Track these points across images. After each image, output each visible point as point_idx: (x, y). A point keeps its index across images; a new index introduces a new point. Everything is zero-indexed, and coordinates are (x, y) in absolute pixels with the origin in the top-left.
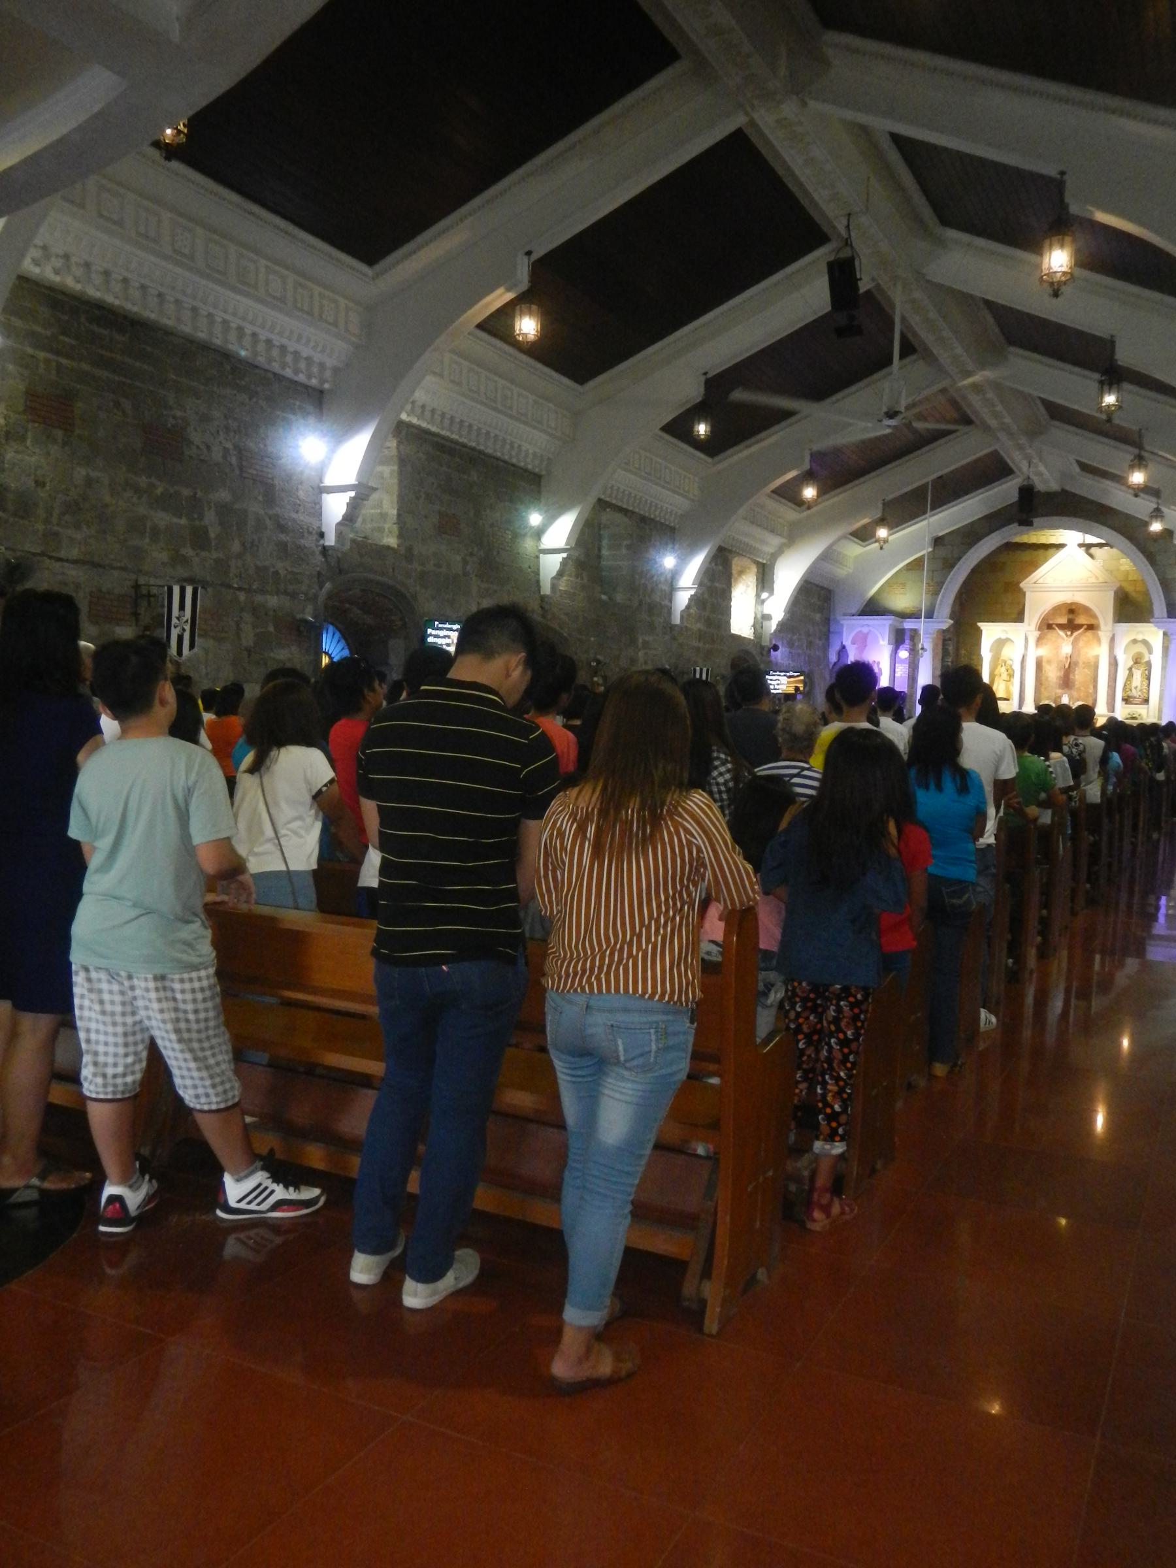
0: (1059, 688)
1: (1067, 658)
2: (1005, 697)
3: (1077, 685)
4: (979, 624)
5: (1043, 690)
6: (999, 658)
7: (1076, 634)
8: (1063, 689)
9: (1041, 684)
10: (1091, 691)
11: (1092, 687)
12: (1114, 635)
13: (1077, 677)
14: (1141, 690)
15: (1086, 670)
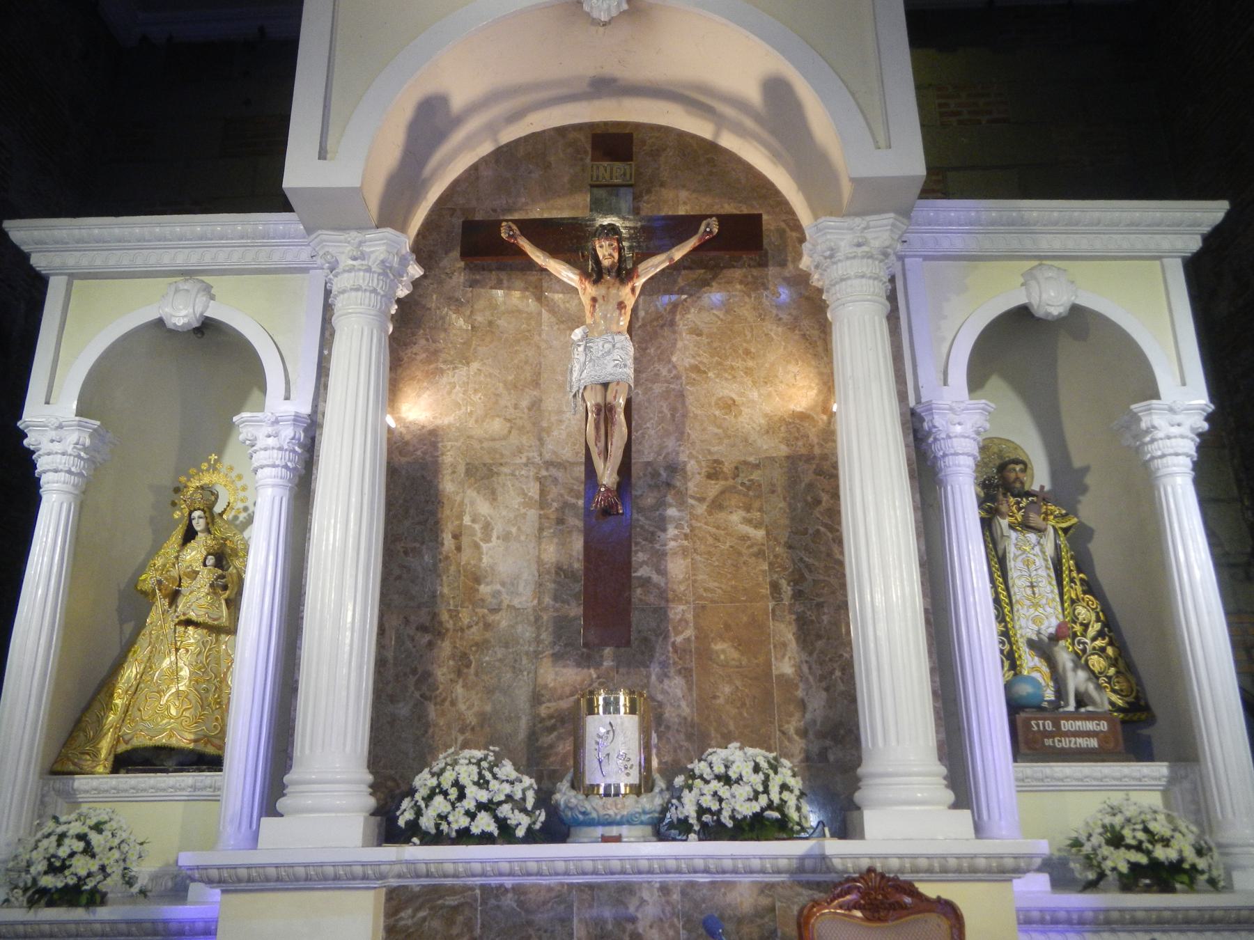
0: (557, 657)
1: (605, 412)
2: (184, 739)
3: (678, 611)
4: (22, 232)
5: (442, 674)
6: (177, 490)
7: (654, 266)
8: (587, 658)
9: (433, 629)
10: (785, 667)
11: (786, 632)
12: (892, 280)
13: (677, 568)
14: (1080, 660)
15: (735, 518)
